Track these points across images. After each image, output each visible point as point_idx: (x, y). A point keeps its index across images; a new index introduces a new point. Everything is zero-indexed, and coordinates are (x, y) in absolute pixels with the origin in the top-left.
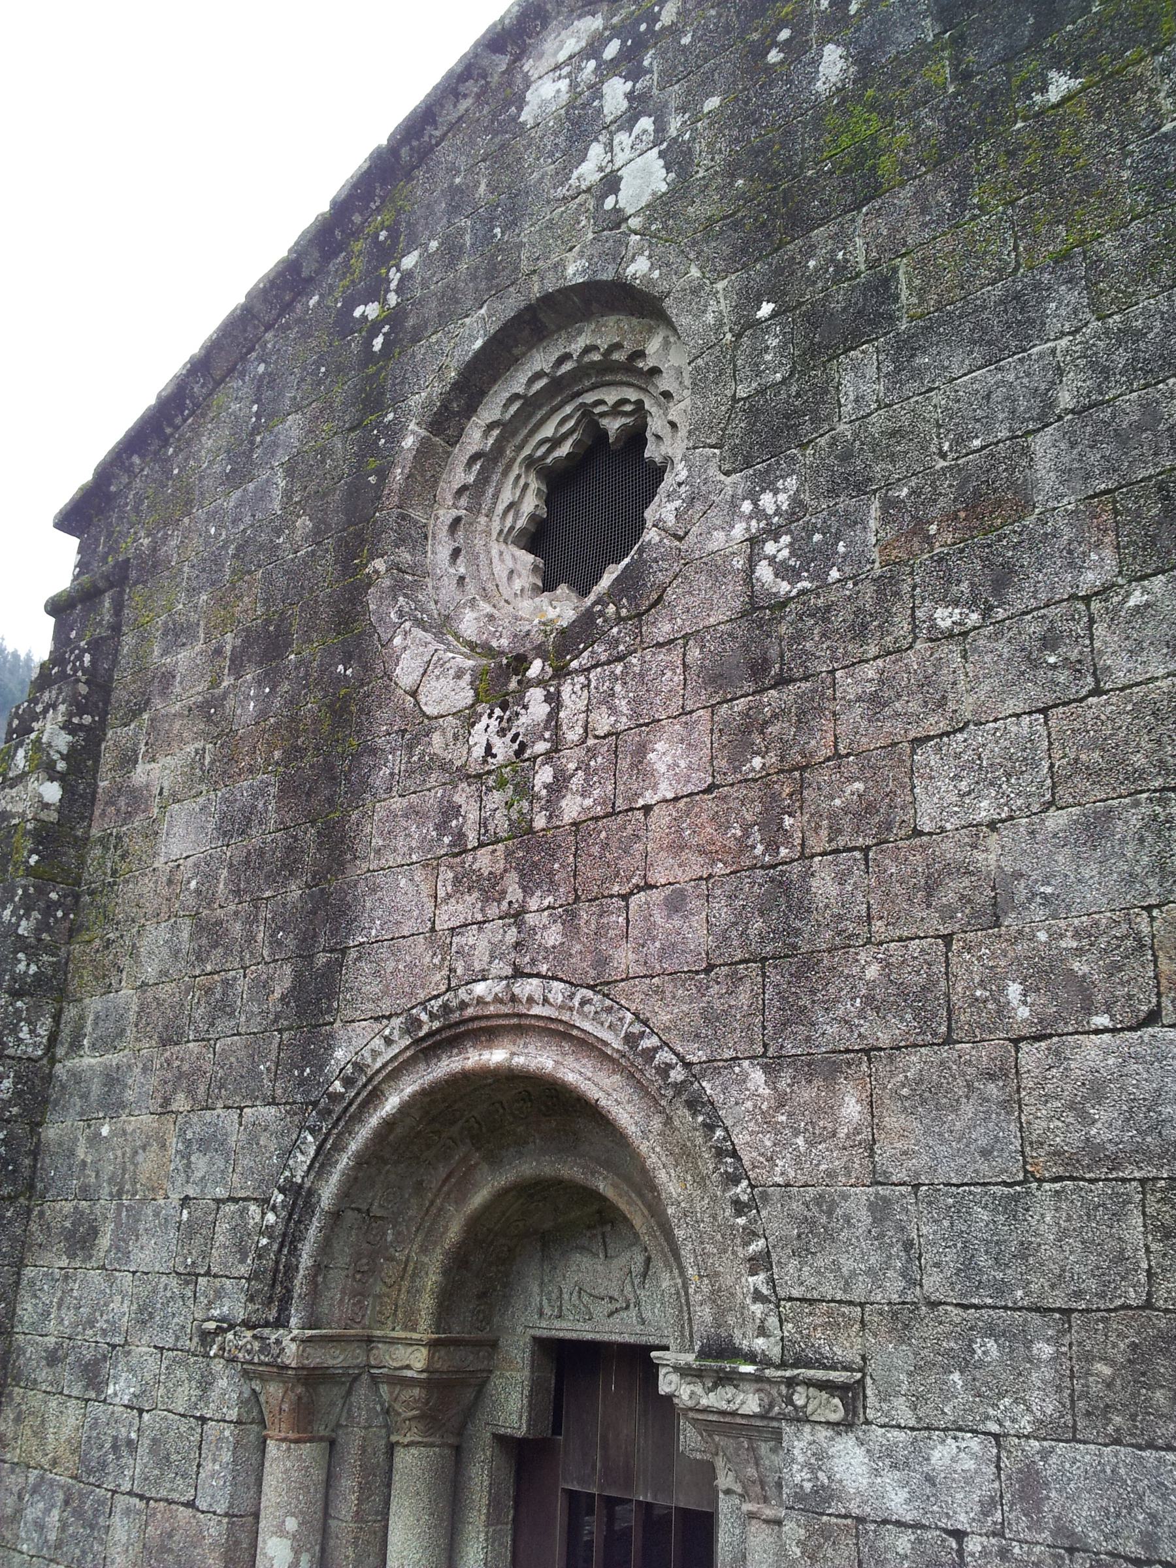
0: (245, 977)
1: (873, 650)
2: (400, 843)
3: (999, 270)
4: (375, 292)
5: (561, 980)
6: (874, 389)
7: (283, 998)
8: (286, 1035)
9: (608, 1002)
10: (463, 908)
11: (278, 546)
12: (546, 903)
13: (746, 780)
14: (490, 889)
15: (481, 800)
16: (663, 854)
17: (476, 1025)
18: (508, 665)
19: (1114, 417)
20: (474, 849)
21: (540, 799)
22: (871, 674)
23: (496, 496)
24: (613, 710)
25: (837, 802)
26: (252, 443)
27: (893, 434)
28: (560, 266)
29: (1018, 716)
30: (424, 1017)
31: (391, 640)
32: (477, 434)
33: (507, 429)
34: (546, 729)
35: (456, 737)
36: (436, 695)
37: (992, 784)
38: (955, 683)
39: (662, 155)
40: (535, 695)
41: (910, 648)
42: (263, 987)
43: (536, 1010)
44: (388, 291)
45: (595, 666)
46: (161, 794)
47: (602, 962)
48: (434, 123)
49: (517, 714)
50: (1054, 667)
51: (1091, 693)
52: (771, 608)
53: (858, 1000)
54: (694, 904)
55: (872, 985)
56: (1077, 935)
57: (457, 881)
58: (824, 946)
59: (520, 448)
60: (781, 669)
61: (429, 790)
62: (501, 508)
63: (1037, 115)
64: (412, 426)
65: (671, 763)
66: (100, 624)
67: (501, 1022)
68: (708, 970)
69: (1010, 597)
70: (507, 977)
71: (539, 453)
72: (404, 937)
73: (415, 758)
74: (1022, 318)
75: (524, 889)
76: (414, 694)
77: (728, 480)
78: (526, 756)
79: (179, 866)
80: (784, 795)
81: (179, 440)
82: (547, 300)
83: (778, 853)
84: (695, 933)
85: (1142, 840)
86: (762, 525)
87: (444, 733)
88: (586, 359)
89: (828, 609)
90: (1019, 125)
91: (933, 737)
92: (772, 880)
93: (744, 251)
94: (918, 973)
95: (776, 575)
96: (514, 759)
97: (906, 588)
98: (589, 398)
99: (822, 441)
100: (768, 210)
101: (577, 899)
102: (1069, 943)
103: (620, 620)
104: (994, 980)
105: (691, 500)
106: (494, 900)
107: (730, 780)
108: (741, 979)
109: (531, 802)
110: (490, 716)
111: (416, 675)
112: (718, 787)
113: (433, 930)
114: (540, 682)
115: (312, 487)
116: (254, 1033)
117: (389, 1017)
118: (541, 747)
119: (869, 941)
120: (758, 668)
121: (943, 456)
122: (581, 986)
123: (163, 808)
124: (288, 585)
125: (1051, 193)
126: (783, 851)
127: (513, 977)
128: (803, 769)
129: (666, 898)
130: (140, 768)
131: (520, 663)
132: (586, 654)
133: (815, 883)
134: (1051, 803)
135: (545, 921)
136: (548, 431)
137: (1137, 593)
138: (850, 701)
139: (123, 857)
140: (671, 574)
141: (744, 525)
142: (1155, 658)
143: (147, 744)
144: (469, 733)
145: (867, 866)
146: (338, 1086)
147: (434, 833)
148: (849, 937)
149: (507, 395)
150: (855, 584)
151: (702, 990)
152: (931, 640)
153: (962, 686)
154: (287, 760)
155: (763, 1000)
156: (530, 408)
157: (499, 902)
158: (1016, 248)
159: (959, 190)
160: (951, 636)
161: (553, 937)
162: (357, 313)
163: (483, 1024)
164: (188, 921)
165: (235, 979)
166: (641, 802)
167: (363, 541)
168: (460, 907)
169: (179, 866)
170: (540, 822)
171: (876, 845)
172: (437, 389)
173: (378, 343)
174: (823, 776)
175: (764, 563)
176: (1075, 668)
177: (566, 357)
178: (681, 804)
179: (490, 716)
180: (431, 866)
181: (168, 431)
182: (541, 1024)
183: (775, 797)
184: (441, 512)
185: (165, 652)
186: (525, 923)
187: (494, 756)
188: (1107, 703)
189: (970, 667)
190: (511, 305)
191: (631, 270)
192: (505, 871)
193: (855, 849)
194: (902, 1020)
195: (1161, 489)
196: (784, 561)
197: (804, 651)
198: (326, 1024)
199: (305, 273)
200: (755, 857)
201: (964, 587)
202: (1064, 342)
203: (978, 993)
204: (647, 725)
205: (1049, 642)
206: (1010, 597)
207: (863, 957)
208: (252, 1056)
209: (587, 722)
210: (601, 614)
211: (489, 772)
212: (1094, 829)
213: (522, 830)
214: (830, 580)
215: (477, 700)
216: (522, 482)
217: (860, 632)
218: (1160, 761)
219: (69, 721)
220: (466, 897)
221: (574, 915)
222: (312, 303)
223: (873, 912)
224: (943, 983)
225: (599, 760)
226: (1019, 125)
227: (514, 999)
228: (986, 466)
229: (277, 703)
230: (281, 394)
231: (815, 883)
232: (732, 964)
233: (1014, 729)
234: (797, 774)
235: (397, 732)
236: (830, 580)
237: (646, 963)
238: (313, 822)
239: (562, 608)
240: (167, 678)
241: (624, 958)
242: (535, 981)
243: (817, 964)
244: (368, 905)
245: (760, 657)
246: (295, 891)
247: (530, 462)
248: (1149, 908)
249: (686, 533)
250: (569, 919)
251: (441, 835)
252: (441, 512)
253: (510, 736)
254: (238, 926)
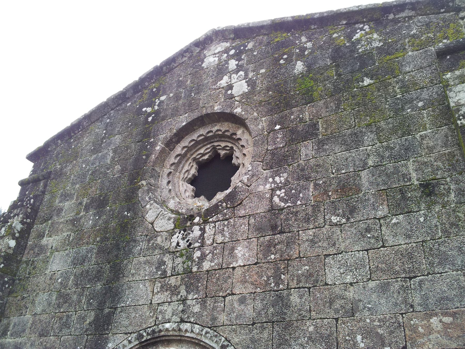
0: (76, 315)
1: (311, 226)
2: (142, 272)
3: (349, 126)
4: (151, 104)
5: (198, 324)
6: (311, 153)
7: (90, 323)
8: (89, 337)
9: (216, 333)
11: (107, 173)
12: (195, 297)
13: (269, 262)
14: (174, 290)
15: (174, 260)
16: (239, 284)
17: (164, 338)
18: (187, 218)
19: (385, 169)
20: (170, 276)
21: (195, 261)
22: (311, 233)
23: (183, 167)
24: (223, 235)
25: (300, 272)
26: (102, 142)
27: (317, 166)
28: (212, 107)
29: (359, 251)
30: (145, 334)
31: (145, 206)
32: (180, 149)
33: (189, 149)
34: (199, 239)
35: (166, 239)
36: (160, 225)
37: (351, 271)
38: (338, 239)
39: (246, 82)
40: (196, 228)
41: (324, 227)
42: (82, 319)
43: (188, 334)
44: (155, 105)
45: (218, 221)
46: (52, 248)
47: (214, 319)
48: (175, 62)
49: (189, 233)
50: (370, 238)
51: (381, 247)
52: (278, 210)
53: (306, 338)
54: (249, 301)
55: (311, 333)
56: (379, 321)
57: (162, 287)
58: (295, 319)
59: (192, 155)
60: (281, 229)
61: (155, 255)
62: (184, 171)
63: (361, 88)
64: (159, 144)
65: (243, 254)
66: (38, 190)
67: (174, 338)
68: (253, 324)
69: (355, 216)
70: (178, 322)
71: (198, 157)
72: (139, 305)
73: (150, 245)
74: (356, 140)
75: (187, 292)
76: (152, 224)
77: (265, 172)
78: (191, 247)
79: (55, 273)
80: (282, 268)
81: (75, 137)
82: (207, 115)
83: (279, 287)
84: (249, 311)
85: (399, 293)
86: (276, 186)
87: (162, 237)
88: (217, 133)
89: (297, 212)
90: (355, 89)
91: (331, 255)
92: (277, 296)
93: (271, 111)
94: (327, 330)
95: (280, 201)
96: (187, 248)
97: (322, 209)
98: (216, 144)
99: (295, 165)
100: (279, 101)
101: (206, 296)
102: (377, 323)
103: (227, 208)
104: (352, 334)
105: (253, 176)
106: (175, 295)
107: (263, 261)
108: (265, 328)
109: (192, 262)
110: (179, 233)
111: (153, 218)
112: (259, 263)
113: (151, 303)
114: (198, 224)
115: (122, 157)
116: (77, 335)
117: (131, 333)
118: (197, 245)
119: (310, 318)
120: (274, 228)
121: (333, 174)
122: (206, 327)
123: (52, 253)
124: (110, 185)
125: (365, 108)
126: (281, 286)
127: (180, 322)
128: (288, 260)
129: (239, 299)
130: (45, 239)
131: (192, 217)
132: (215, 217)
133: (292, 298)
134: (370, 279)
135: (194, 303)
136: (202, 151)
137: (395, 219)
138: (304, 241)
139: (34, 268)
140: (245, 196)
141: (270, 185)
142: (401, 239)
143: (49, 231)
144: (171, 238)
145: (310, 294)
147: (155, 270)
148: (303, 317)
149: (191, 139)
150: (306, 206)
151: (251, 331)
152: (330, 225)
153: (340, 240)
154: (102, 241)
155: (273, 336)
156: (197, 144)
157: (177, 295)
158: (355, 121)
159: (337, 104)
160: (337, 225)
161: (197, 309)
162: (144, 109)
163: (167, 338)
164: (56, 293)
165: (71, 315)
166: (232, 266)
167: (139, 175)
168: (162, 296)
169: (55, 273)
170: (195, 269)
171: (313, 287)
172: (169, 134)
173: (150, 119)
174: (295, 263)
175: (276, 197)
176: (377, 239)
177: (212, 131)
178: (246, 267)
179: (179, 233)
180: (153, 281)
181: (72, 134)
182: (189, 339)
183: (279, 268)
184: (165, 170)
185: (60, 202)
186: (186, 303)
187: (180, 246)
188: (387, 250)
189: (343, 235)
190: (196, 115)
191: (235, 111)
192: (181, 285)
193: (305, 287)
194: (321, 345)
195: (400, 191)
196: (282, 197)
197: (289, 224)
198: (106, 334)
199: (127, 96)
200: (271, 287)
201: (341, 211)
202: (370, 148)
203: (347, 338)
204: (235, 241)
205: (368, 230)
206: (355, 216)
207: (308, 324)
208: (75, 343)
209: (214, 238)
210: (221, 205)
211: (177, 251)
212: (384, 288)
213: (188, 271)
214: (297, 204)
215: (175, 228)
216: (191, 165)
217: (307, 220)
218: (404, 269)
219: (23, 220)
220: (165, 293)
221: (205, 302)
222: (128, 105)
223: (312, 309)
224: (335, 334)
225: (218, 251)
226: (355, 89)
227: (180, 330)
228: (346, 178)
229: (101, 222)
230: (114, 129)
231: (292, 298)
232: (262, 323)
233: (358, 255)
234: (286, 262)
235: (144, 235)
236: (297, 204)
237: (230, 320)
238: (109, 263)
239: (203, 203)
240: (60, 210)
241: (222, 318)
242: (189, 324)
243: (292, 325)
244: (127, 293)
245: (274, 224)
246: (99, 286)
247: (194, 159)
248: (402, 314)
249: (251, 185)
250: (203, 303)
251: (157, 271)
252: (165, 170)
253: (186, 240)
254: (75, 296)
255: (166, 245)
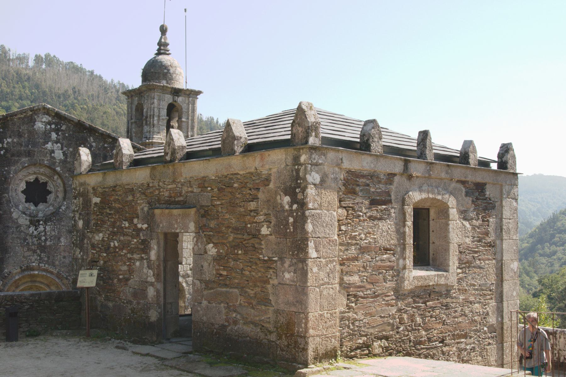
10: (29, 253)
14: (34, 252)
98: (39, 176)
105: (67, 208)
118: (43, 234)
146: (6, 275)
161: (46, 259)
170: (43, 244)
213: (39, 244)
241: (57, 263)
250: (48, 257)
255: (26, 231)
